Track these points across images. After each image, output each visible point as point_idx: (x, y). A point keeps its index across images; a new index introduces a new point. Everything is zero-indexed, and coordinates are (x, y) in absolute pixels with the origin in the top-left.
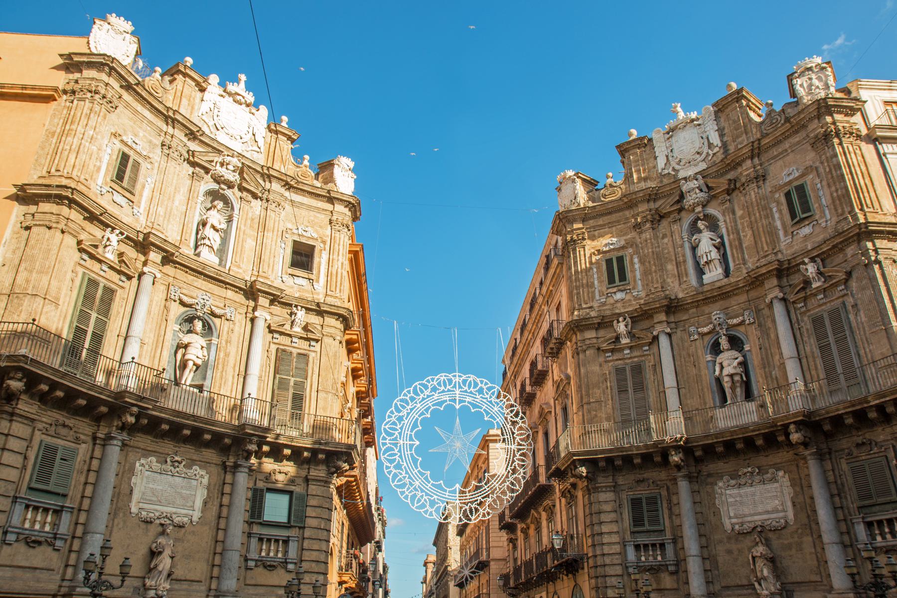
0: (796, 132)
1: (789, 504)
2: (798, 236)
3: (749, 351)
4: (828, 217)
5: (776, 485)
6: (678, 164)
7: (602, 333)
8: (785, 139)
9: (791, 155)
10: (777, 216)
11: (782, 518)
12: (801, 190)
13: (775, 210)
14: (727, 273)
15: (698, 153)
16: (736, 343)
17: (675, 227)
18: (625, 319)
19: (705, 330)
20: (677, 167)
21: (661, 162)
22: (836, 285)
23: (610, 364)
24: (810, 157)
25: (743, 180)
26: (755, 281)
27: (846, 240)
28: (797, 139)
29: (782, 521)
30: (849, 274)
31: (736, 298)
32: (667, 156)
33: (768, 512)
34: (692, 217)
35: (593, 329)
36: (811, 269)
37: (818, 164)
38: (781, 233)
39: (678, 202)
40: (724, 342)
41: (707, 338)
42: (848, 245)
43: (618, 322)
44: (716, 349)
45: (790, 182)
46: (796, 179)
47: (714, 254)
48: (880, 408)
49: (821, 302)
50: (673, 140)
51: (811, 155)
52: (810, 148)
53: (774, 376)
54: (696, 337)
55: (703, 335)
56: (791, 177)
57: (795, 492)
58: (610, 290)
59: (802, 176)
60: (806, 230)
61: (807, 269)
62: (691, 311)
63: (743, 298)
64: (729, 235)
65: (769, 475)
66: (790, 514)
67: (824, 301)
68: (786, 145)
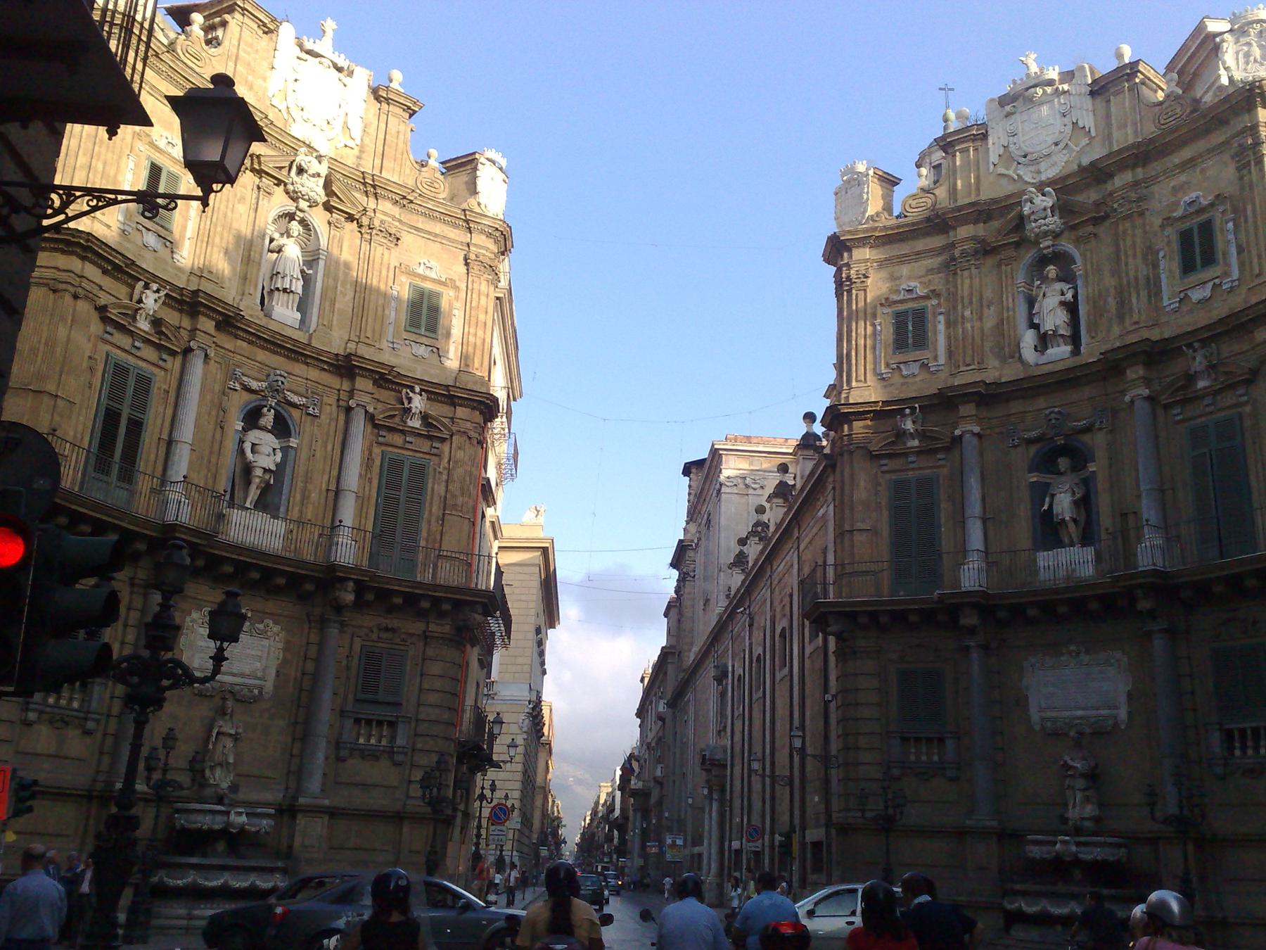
0: (455, 226)
1: (273, 672)
5: (266, 642)
7: (107, 282)
11: (255, 686)
14: (302, 322)
16: (282, 428)
18: (158, 291)
19: (254, 385)
22: (430, 437)
23: (108, 347)
25: (377, 223)
26: (346, 367)
29: (256, 692)
31: (304, 367)
33: (242, 675)
34: (291, 207)
35: (99, 267)
37: (463, 286)
38: (391, 328)
40: (268, 419)
41: (246, 396)
43: (147, 286)
44: (252, 419)
45: (425, 278)
46: (434, 281)
47: (298, 286)
48: (436, 601)
52: (462, 258)
54: (238, 387)
55: (247, 389)
56: (428, 273)
57: (284, 659)
59: (443, 284)
60: (422, 351)
61: (410, 400)
62: (239, 342)
63: (314, 374)
64: (326, 275)
65: (261, 626)
66: (269, 686)
68: (438, 228)
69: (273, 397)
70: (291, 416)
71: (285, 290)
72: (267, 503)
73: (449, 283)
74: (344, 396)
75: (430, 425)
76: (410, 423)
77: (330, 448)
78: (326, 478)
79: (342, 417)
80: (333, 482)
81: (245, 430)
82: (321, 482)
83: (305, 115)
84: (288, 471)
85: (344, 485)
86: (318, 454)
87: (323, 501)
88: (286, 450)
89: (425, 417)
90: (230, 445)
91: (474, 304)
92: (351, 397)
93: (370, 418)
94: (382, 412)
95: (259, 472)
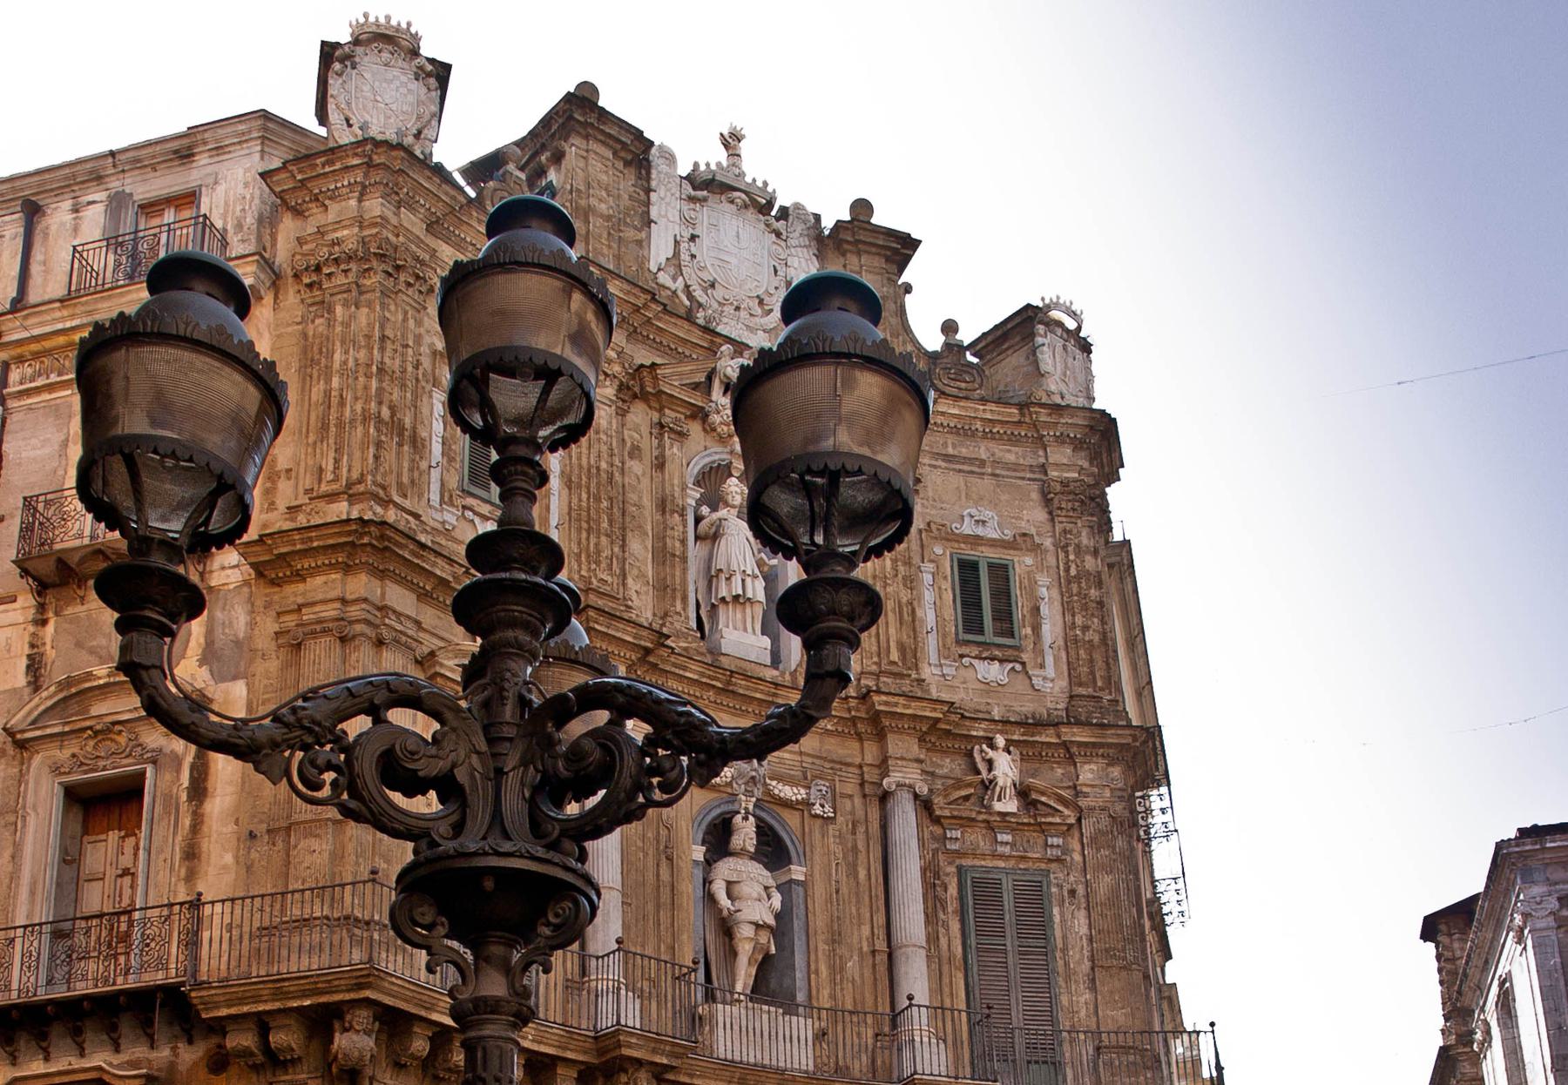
0: (1014, 440)
2: (969, 674)
3: (797, 882)
4: (1050, 671)
6: (705, 290)
8: (985, 435)
9: (988, 481)
10: (928, 596)
12: (1001, 572)
13: (927, 578)
15: (761, 302)
16: (772, 850)
17: (674, 451)
20: (698, 294)
21: (660, 250)
24: (1034, 516)
27: (1094, 745)
28: (1011, 458)
30: (1079, 820)
32: (677, 243)
36: (1006, 769)
37: (1048, 543)
39: (696, 386)
40: (745, 834)
42: (1088, 759)
45: (976, 540)
46: (993, 543)
49: (1000, 849)
50: (704, 215)
51: (1040, 515)
52: (1035, 496)
53: (849, 974)
56: (980, 531)
58: (470, 501)
60: (993, 672)
61: (990, 764)
67: (1007, 850)
68: (983, 451)
69: (749, 793)
70: (783, 824)
71: (736, 597)
72: (770, 986)
73: (1022, 542)
74: (871, 775)
75: (1035, 803)
76: (998, 806)
77: (862, 874)
78: (866, 930)
79: (874, 815)
80: (882, 933)
81: (709, 863)
82: (862, 935)
83: (719, 293)
84: (797, 924)
85: (899, 936)
86: (844, 890)
87: (868, 973)
88: (785, 888)
89: (1023, 793)
90: (690, 889)
91: (1073, 572)
92: (885, 774)
93: (925, 805)
94: (946, 792)
95: (746, 931)
